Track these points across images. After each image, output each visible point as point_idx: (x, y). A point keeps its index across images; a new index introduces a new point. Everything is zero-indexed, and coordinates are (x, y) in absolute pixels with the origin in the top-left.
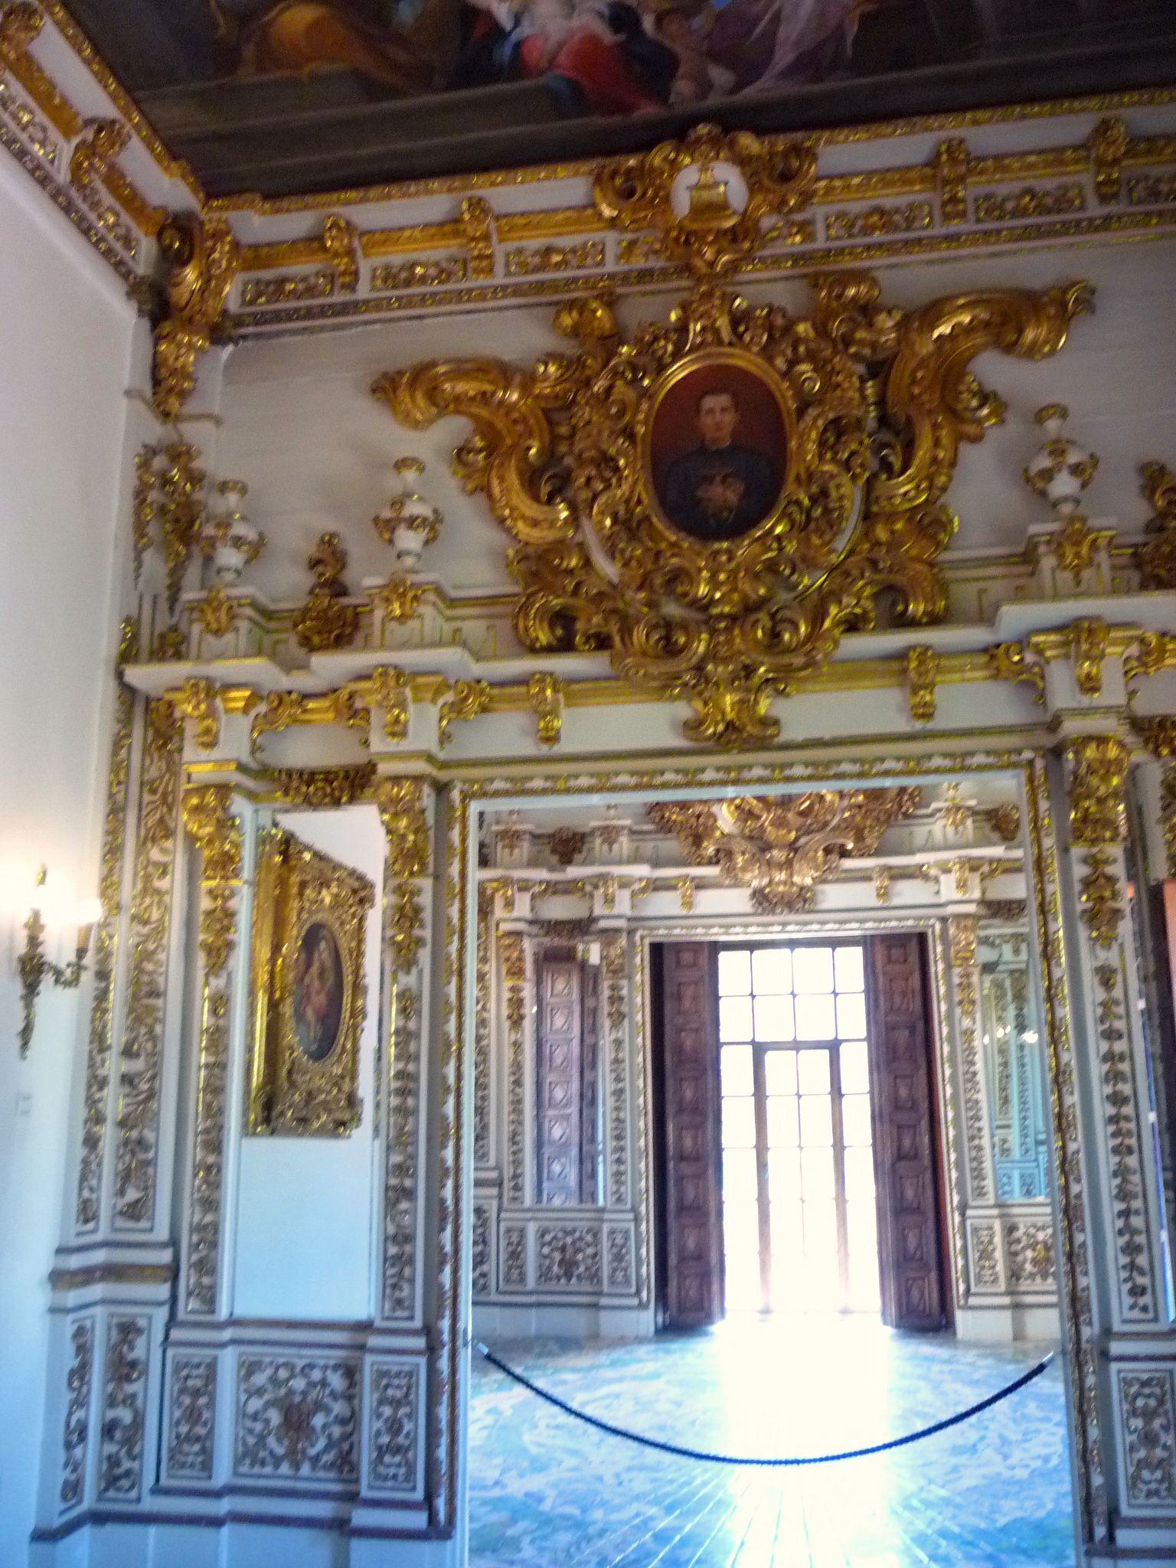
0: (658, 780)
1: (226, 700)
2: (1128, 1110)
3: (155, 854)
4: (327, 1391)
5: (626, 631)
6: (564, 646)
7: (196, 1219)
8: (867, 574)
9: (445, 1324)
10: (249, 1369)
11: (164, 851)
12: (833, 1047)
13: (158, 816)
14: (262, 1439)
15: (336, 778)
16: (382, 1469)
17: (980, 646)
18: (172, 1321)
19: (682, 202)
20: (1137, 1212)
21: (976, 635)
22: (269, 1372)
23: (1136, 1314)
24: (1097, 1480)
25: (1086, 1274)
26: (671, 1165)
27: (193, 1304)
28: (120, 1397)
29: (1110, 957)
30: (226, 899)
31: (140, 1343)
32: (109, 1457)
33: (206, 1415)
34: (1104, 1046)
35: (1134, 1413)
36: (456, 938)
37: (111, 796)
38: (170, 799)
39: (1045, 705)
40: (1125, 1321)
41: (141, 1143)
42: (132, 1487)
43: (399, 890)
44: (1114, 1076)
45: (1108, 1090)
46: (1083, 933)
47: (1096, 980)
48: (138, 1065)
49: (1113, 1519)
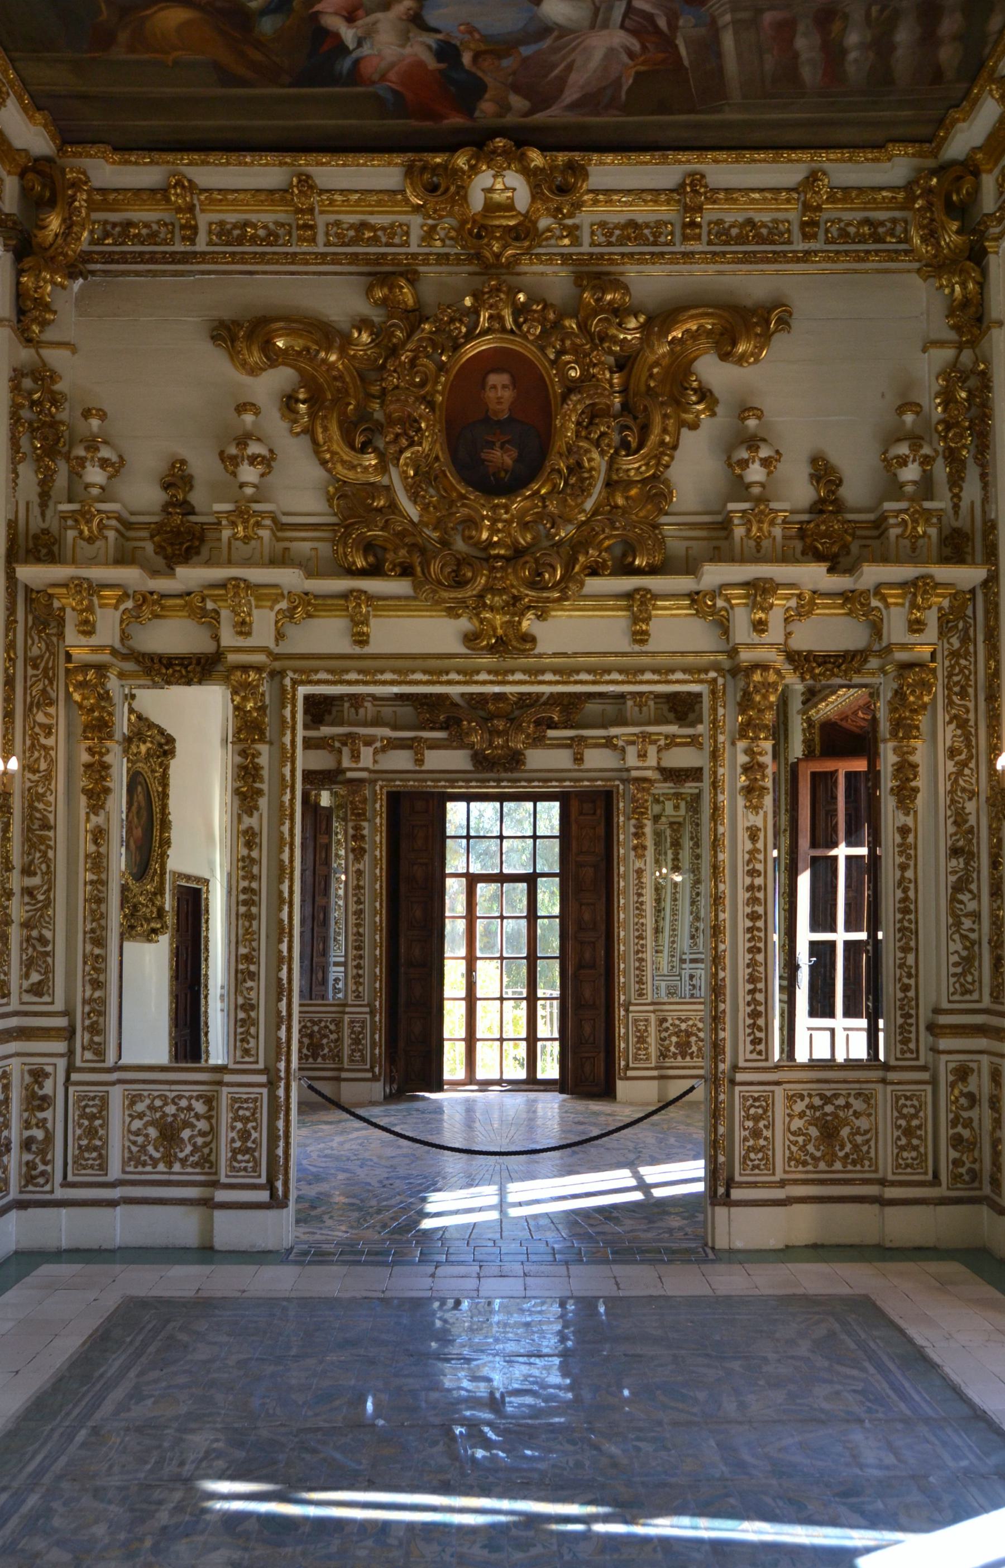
0: (444, 678)
1: (101, 597)
2: (760, 924)
3: (40, 718)
4: (192, 1114)
5: (425, 565)
6: (374, 571)
7: (88, 994)
8: (607, 530)
9: (282, 1065)
10: (133, 1100)
11: (46, 714)
13: (41, 687)
14: (143, 1148)
15: (190, 664)
16: (235, 1164)
17: (686, 592)
18: (70, 1069)
19: (477, 202)
20: (760, 991)
21: (683, 583)
22: (148, 1102)
23: (754, 1056)
24: (721, 1159)
25: (724, 1030)
27: (89, 1055)
28: (34, 1121)
29: (758, 821)
30: (101, 755)
31: (48, 1084)
32: (27, 1163)
33: (101, 1132)
34: (748, 881)
35: (748, 1117)
36: (288, 791)
37: (6, 669)
38: (51, 673)
39: (728, 639)
40: (746, 1061)
41: (43, 940)
42: (47, 1182)
43: (243, 753)
44: (753, 901)
45: (748, 910)
46: (741, 802)
47: (746, 835)
48: (36, 881)
49: (730, 1183)
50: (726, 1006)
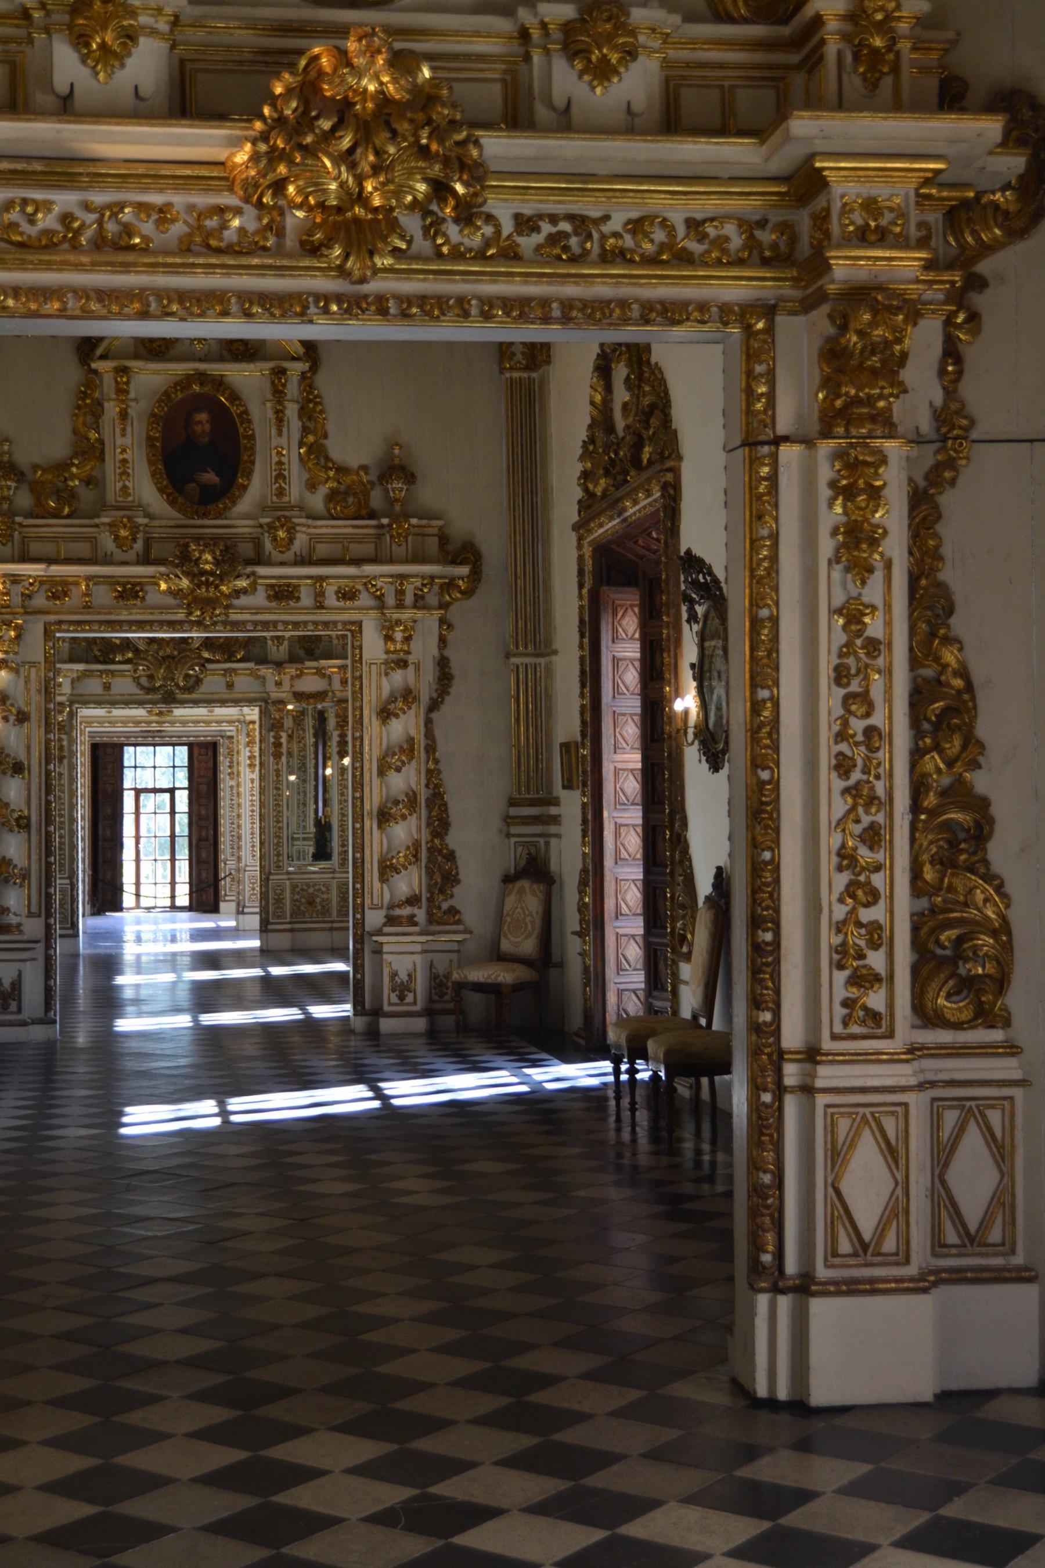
12: (172, 791)
26: (100, 843)
46: (248, 769)
49: (244, 907)
50: (243, 843)
